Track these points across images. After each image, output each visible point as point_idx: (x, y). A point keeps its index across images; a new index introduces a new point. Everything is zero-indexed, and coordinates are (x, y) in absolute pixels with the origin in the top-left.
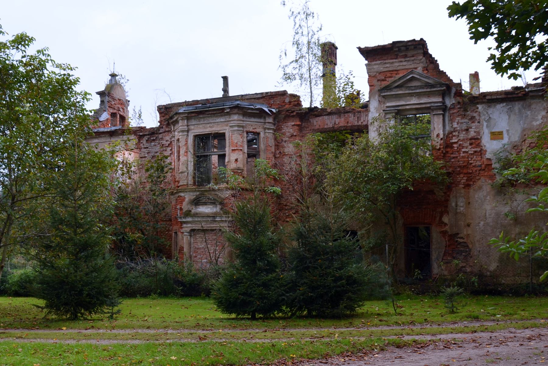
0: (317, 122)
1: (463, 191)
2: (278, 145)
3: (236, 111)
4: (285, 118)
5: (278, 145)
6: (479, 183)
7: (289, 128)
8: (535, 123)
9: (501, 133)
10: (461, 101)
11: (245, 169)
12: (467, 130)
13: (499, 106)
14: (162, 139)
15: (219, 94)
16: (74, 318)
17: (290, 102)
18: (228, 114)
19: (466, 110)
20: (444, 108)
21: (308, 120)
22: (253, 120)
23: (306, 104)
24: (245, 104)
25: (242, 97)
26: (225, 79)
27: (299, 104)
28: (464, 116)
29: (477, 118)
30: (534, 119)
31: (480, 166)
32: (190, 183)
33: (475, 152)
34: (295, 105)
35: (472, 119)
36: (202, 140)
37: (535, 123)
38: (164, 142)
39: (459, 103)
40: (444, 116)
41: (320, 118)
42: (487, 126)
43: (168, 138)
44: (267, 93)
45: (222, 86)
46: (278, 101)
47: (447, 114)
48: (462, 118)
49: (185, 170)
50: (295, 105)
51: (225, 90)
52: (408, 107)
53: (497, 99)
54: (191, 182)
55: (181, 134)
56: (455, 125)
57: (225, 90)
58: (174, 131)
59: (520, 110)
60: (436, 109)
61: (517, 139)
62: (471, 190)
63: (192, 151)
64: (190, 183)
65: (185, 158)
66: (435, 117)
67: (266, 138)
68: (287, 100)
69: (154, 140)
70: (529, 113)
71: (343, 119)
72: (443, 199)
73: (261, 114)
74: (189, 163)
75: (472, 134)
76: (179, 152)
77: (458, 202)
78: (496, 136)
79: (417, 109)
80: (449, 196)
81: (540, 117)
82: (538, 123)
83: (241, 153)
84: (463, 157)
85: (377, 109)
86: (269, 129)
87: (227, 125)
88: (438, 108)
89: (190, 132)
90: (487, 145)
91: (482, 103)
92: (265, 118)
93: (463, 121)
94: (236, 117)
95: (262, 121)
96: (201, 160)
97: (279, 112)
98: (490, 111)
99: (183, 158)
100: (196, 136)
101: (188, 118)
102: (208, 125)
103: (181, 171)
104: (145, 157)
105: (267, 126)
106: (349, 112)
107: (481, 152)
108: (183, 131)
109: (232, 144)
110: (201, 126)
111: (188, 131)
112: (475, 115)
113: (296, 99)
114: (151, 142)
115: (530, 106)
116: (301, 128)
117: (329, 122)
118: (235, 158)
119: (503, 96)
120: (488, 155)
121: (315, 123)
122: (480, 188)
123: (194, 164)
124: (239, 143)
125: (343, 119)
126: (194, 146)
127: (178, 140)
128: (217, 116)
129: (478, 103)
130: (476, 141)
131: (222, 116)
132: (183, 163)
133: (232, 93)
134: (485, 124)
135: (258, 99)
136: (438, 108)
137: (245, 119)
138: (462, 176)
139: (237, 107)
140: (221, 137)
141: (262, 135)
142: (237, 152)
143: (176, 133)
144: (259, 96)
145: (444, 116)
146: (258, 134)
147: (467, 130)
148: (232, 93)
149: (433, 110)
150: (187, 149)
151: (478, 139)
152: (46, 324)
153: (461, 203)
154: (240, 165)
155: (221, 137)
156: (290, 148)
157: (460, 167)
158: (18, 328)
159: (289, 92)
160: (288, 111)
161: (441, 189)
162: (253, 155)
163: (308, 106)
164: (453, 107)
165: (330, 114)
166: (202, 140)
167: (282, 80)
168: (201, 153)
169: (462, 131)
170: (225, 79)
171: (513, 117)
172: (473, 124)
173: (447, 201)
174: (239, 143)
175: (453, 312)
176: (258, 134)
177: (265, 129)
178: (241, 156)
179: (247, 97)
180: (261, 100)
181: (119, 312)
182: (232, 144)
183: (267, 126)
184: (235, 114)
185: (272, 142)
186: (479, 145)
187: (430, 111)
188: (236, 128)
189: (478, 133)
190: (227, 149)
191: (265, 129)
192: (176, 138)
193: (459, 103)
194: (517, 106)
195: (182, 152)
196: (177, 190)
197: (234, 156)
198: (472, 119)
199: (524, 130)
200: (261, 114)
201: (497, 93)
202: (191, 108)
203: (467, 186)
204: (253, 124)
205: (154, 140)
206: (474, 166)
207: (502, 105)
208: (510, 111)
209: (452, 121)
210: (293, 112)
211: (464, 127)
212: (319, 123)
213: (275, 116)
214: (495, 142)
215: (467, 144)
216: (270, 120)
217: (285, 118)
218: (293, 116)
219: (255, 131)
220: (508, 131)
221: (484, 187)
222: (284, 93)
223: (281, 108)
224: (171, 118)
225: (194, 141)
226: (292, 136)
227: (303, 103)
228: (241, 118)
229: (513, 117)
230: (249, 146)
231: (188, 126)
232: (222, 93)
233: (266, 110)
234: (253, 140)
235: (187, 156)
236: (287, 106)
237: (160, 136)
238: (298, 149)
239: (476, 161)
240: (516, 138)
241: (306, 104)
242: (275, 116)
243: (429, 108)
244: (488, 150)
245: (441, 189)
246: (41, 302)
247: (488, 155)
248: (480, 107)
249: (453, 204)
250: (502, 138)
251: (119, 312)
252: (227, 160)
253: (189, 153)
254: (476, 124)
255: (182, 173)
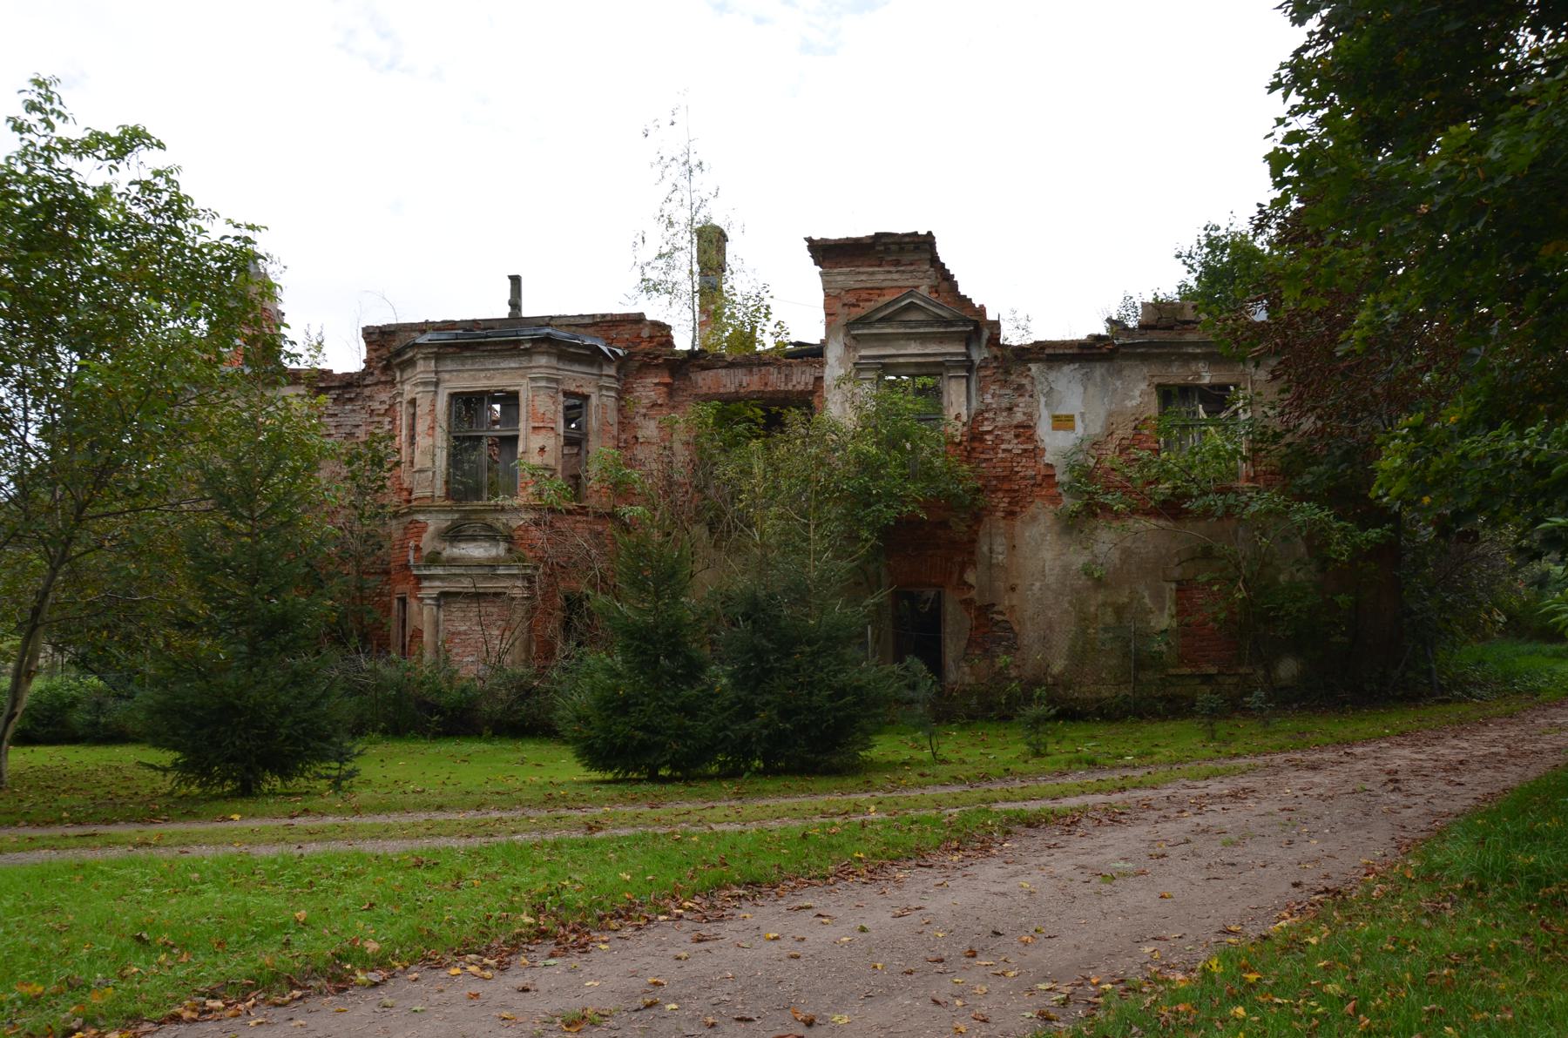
0: (705, 381)
1: (1002, 524)
2: (625, 423)
3: (544, 347)
4: (639, 370)
5: (625, 423)
6: (1032, 509)
7: (648, 389)
8: (1129, 404)
9: (1070, 418)
10: (999, 354)
11: (559, 468)
12: (1010, 409)
13: (1067, 369)
14: (370, 398)
15: (503, 312)
16: (247, 790)
17: (651, 338)
18: (528, 353)
19: (1007, 372)
20: (969, 366)
21: (686, 376)
22: (576, 368)
23: (683, 341)
24: (561, 334)
25: (549, 321)
26: (516, 281)
27: (669, 342)
28: (1005, 383)
29: (1029, 387)
30: (1127, 396)
31: (1034, 477)
32: (438, 493)
33: (1025, 451)
34: (662, 345)
35: (1020, 389)
36: (468, 404)
37: (1129, 404)
38: (375, 405)
39: (996, 358)
40: (968, 379)
41: (711, 373)
42: (1047, 404)
43: (384, 396)
44: (604, 316)
45: (508, 297)
46: (626, 333)
47: (974, 378)
48: (1002, 387)
49: (429, 464)
50: (662, 345)
51: (515, 304)
52: (901, 360)
53: (1065, 355)
54: (440, 491)
55: (420, 389)
56: (988, 399)
57: (515, 304)
58: (402, 383)
59: (1103, 379)
60: (954, 367)
61: (1098, 430)
62: (1018, 523)
63: (445, 425)
64: (438, 493)
65: (430, 441)
66: (953, 383)
67: (602, 407)
68: (645, 333)
69: (351, 400)
70: (1118, 383)
71: (756, 378)
72: (965, 538)
73: (593, 357)
74: (438, 451)
75: (1019, 417)
76: (412, 427)
77: (994, 545)
78: (1063, 422)
79: (917, 364)
80: (976, 533)
81: (1137, 393)
82: (1134, 403)
83: (552, 434)
84: (1003, 460)
85: (841, 361)
86: (608, 388)
87: (523, 377)
88: (957, 365)
89: (442, 386)
90: (1047, 440)
91: (1036, 361)
92: (600, 366)
93: (1003, 392)
94: (543, 360)
95: (595, 371)
96: (461, 446)
97: (630, 356)
98: (1052, 376)
99: (422, 441)
100: (454, 396)
101: (438, 357)
102: (483, 374)
103: (417, 467)
104: (330, 435)
105: (605, 382)
106: (769, 364)
107: (1035, 452)
108: (425, 384)
109: (533, 415)
110: (466, 375)
111: (437, 384)
112: (1025, 381)
113: (662, 332)
114: (344, 404)
115: (1120, 371)
116: (671, 391)
117: (729, 382)
118: (538, 445)
119: (1075, 351)
120: (1049, 458)
121: (700, 382)
122: (1034, 518)
123: (449, 455)
124: (549, 415)
125: (756, 378)
126: (450, 415)
127: (413, 402)
128: (502, 357)
129: (1030, 361)
130: (1025, 430)
131: (512, 356)
132: (426, 452)
133: (527, 312)
134: (1043, 400)
135: (585, 326)
136: (957, 365)
137: (560, 366)
138: (1000, 495)
139: (547, 339)
140: (510, 400)
141: (594, 400)
142: (543, 432)
143: (407, 387)
144: (587, 321)
145: (968, 379)
146: (586, 398)
147: (1010, 409)
148: (527, 312)
149: (948, 369)
150: (434, 421)
151: (1029, 427)
152: (184, 808)
153: (1000, 545)
154: (549, 459)
155: (510, 400)
156: (649, 429)
157: (997, 478)
158: (115, 822)
159: (650, 316)
160: (647, 354)
161: (962, 520)
162: (575, 441)
163: (687, 347)
164: (985, 364)
165: (731, 365)
166: (468, 404)
167: (636, 292)
168: (465, 430)
169: (1001, 410)
170: (516, 281)
171: (1091, 390)
172: (1021, 399)
173: (973, 541)
174: (549, 415)
175: (1038, 754)
176: (586, 398)
177: (601, 388)
178: (552, 442)
179: (565, 322)
180: (590, 330)
181: (351, 774)
182: (533, 415)
183: (605, 382)
184: (542, 353)
185: (613, 416)
186: (1030, 439)
187: (942, 370)
188: (543, 384)
189: (1030, 416)
190: (522, 425)
191: (601, 388)
192: (407, 397)
193: (996, 358)
194: (1099, 370)
195: (421, 427)
196: (410, 507)
197: (537, 441)
198: (1020, 389)
199: (1110, 414)
200: (593, 357)
201: (1064, 344)
202: (444, 336)
203: (1010, 514)
204: (577, 378)
205: (351, 400)
206: (1023, 478)
207: (1072, 367)
208: (1087, 377)
209: (982, 390)
210: (657, 357)
211: (1005, 403)
212: (709, 382)
213: (622, 363)
214: (1061, 433)
215: (1009, 436)
216: (612, 371)
217: (639, 370)
218: (657, 366)
219: (580, 390)
220: (1082, 414)
221: (1041, 517)
222: (638, 319)
223: (618, 349)
224: (399, 353)
225: (450, 405)
226: (654, 405)
227: (676, 341)
228: (554, 362)
229: (1091, 390)
230: (568, 421)
231: (437, 372)
232: (508, 309)
233: (605, 349)
234: (576, 407)
235: (432, 436)
236: (643, 345)
237: (367, 392)
238: (665, 436)
239: (1026, 469)
240: (1096, 429)
241: (683, 341)
242: (622, 363)
243: (941, 364)
244: (1048, 449)
245: (962, 520)
246: (166, 757)
247: (1049, 458)
248: (1034, 367)
249: (985, 549)
250: (1073, 428)
251: (351, 774)
252: (520, 449)
253: (438, 430)
254: (1027, 398)
255: (420, 471)
